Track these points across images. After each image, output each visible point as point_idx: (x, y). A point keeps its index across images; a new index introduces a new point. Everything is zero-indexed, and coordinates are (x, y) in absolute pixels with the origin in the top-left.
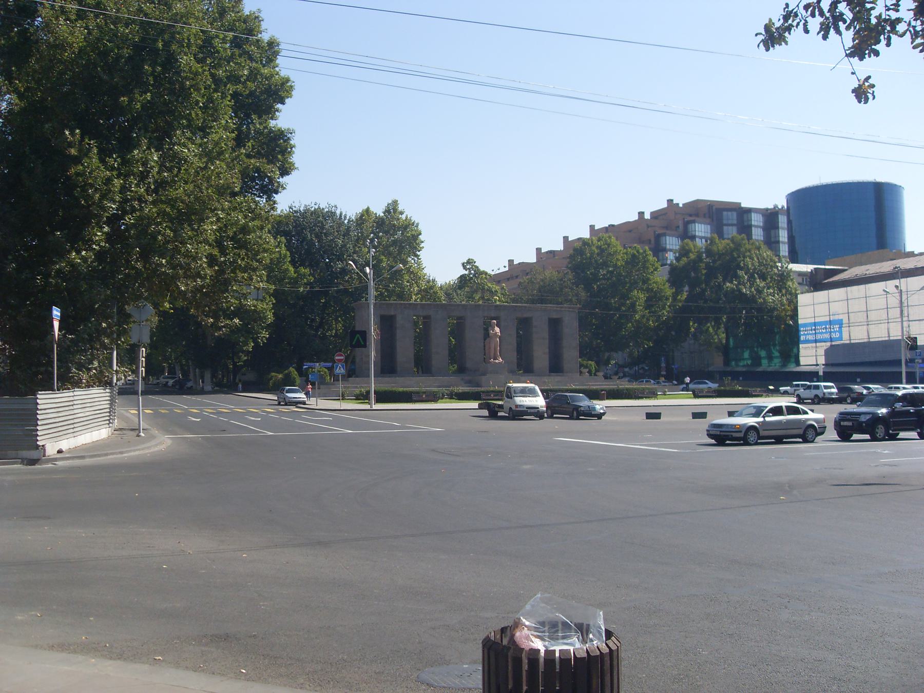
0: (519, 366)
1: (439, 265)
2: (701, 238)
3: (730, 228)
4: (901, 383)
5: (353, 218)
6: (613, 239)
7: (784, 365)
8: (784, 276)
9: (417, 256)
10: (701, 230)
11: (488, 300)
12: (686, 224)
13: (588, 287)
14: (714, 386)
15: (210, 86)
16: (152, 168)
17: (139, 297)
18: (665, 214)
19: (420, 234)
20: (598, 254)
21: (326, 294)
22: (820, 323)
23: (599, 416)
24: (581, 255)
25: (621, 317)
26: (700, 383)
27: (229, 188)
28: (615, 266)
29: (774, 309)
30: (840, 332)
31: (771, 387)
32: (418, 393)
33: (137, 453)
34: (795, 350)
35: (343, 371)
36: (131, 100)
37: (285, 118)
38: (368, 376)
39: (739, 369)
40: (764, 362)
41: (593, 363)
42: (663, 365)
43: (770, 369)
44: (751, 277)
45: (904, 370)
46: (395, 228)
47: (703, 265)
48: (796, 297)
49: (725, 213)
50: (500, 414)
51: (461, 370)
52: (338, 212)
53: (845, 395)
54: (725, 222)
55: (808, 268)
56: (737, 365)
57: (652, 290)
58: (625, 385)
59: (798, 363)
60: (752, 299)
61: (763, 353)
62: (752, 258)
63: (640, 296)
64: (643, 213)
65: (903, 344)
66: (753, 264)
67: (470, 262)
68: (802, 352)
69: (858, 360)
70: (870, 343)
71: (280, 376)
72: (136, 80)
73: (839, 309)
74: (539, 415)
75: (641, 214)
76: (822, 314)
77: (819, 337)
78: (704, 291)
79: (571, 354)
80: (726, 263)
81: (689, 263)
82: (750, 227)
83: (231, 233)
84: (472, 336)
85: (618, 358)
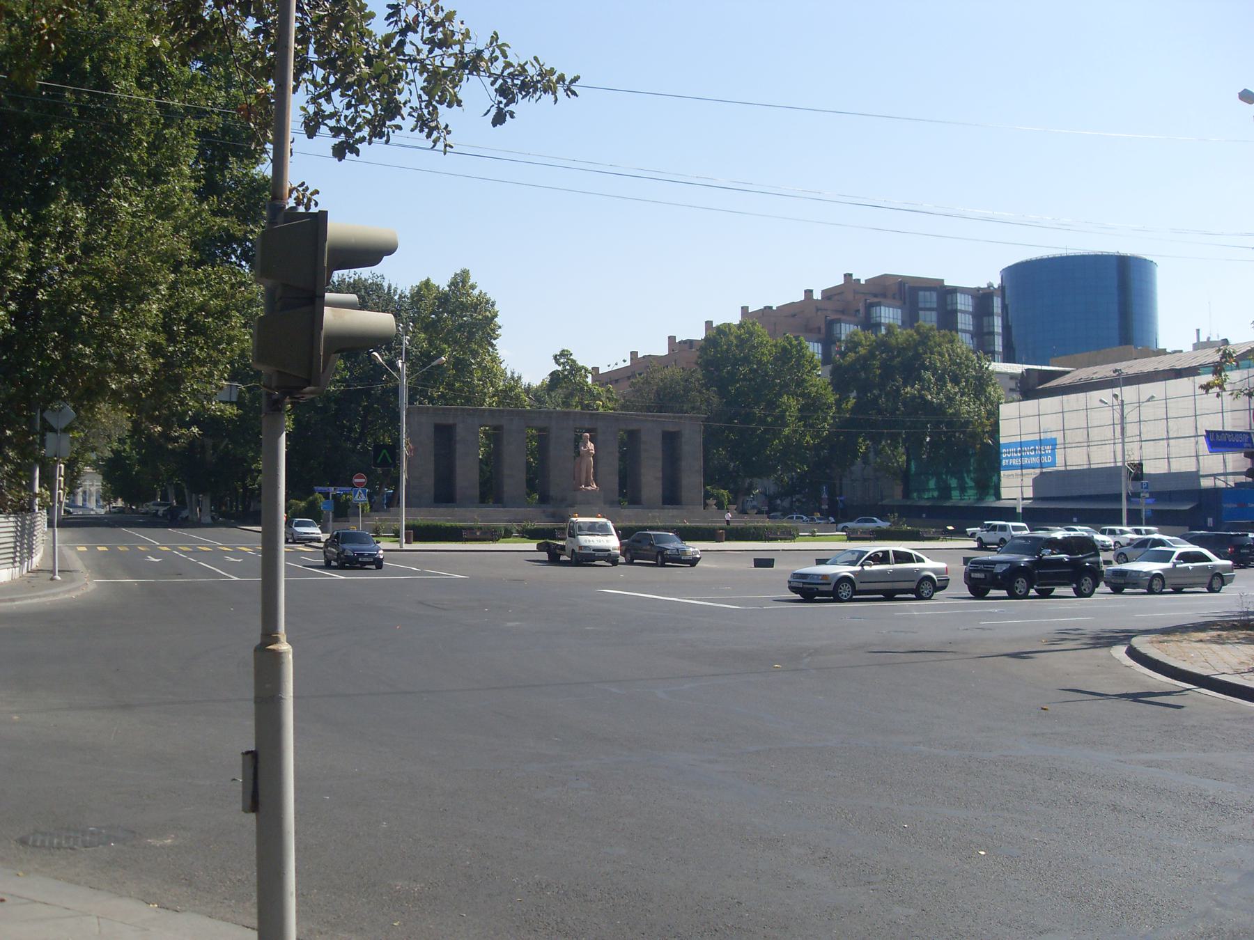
0: (622, 494)
1: (523, 358)
3: (928, 313)
4: (1120, 524)
5: (407, 293)
7: (981, 499)
9: (492, 345)
10: (889, 315)
11: (588, 406)
13: (722, 392)
14: (884, 525)
15: (158, 121)
16: (76, 227)
17: (57, 397)
19: (496, 316)
20: (737, 346)
21: (367, 393)
23: (693, 562)
24: (715, 347)
25: (766, 431)
26: (866, 521)
27: (173, 255)
28: (759, 362)
29: (967, 423)
31: (950, 528)
32: (470, 529)
33: (36, 600)
34: (995, 479)
36: (47, 139)
39: (922, 503)
40: (955, 494)
41: (725, 492)
43: (962, 504)
44: (941, 379)
45: (1124, 506)
46: (464, 307)
47: (877, 363)
49: (921, 293)
50: (562, 558)
51: (544, 499)
52: (386, 285)
54: (921, 305)
55: (1017, 369)
56: (920, 498)
58: (764, 522)
59: (998, 496)
62: (941, 354)
63: (791, 404)
64: (811, 291)
65: (1124, 473)
66: (942, 362)
67: (564, 354)
68: (1004, 482)
71: (303, 504)
72: (52, 111)
73: (1051, 424)
74: (614, 561)
75: (809, 293)
77: (1025, 461)
79: (692, 479)
80: (907, 361)
81: (858, 359)
82: (954, 312)
83: (184, 315)
85: (762, 486)
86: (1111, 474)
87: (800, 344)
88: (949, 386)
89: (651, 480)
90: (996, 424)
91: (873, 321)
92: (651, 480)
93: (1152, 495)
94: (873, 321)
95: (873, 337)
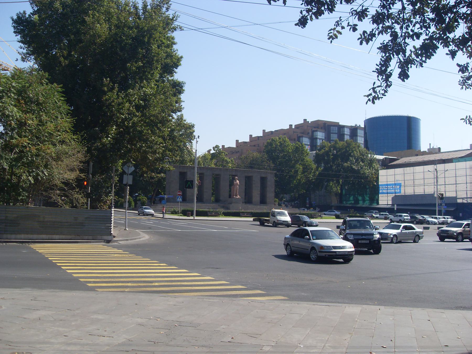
2: (320, 139)
6: (287, 139)
8: (372, 161)
9: (191, 142)
10: (320, 135)
12: (313, 132)
18: (302, 126)
19: (194, 132)
22: (390, 185)
24: (271, 146)
29: (368, 176)
30: (400, 189)
34: (377, 197)
37: (179, 75)
38: (193, 201)
39: (348, 205)
40: (361, 202)
42: (308, 202)
43: (364, 206)
45: (437, 209)
48: (378, 171)
49: (332, 127)
50: (266, 224)
51: (217, 200)
53: (413, 220)
54: (332, 132)
55: (381, 157)
57: (305, 164)
59: (378, 203)
60: (358, 172)
63: (300, 167)
64: (292, 125)
68: (380, 198)
69: (408, 203)
70: (425, 194)
72: (134, 56)
73: (399, 178)
75: (291, 126)
76: (391, 180)
77: (389, 191)
78: (331, 166)
79: (270, 194)
82: (344, 134)
84: (224, 185)
85: (287, 197)
86: (432, 195)
87: (302, 146)
88: (361, 163)
89: (256, 195)
90: (378, 178)
91: (314, 137)
92: (256, 195)
93: (446, 204)
94: (314, 137)
95: (329, 144)
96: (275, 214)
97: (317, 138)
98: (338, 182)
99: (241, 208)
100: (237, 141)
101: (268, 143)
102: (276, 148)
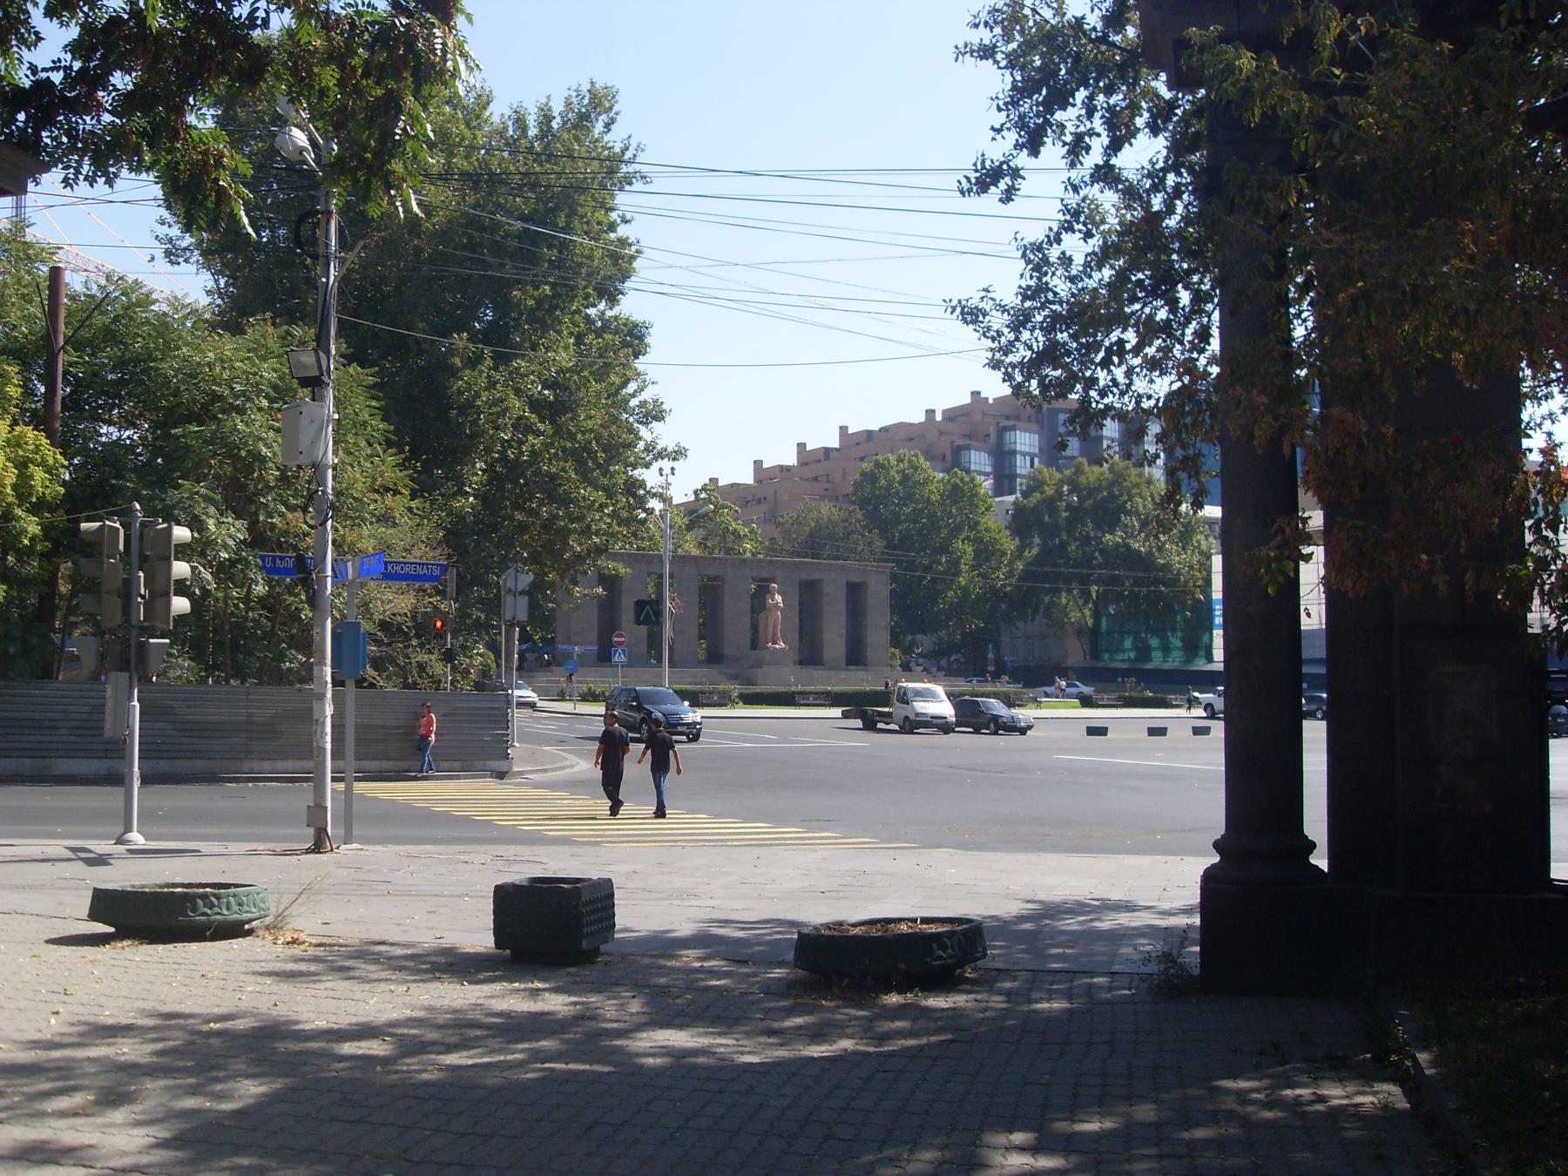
2: (1024, 454)
6: (922, 460)
7: (1188, 661)
12: (1002, 431)
20: (900, 483)
24: (873, 484)
25: (934, 581)
34: (1206, 638)
35: (623, 659)
37: (632, 305)
40: (1157, 656)
42: (990, 656)
43: (1166, 666)
50: (880, 725)
51: (715, 657)
61: (1155, 642)
62: (1144, 499)
63: (965, 549)
64: (933, 411)
74: (945, 728)
75: (930, 413)
78: (1064, 545)
84: (736, 611)
85: (925, 642)
87: (972, 480)
94: (1006, 448)
95: (1058, 476)
96: (910, 695)
97: (1014, 453)
98: (1086, 595)
99: (791, 678)
100: (758, 464)
101: (863, 474)
102: (888, 488)
